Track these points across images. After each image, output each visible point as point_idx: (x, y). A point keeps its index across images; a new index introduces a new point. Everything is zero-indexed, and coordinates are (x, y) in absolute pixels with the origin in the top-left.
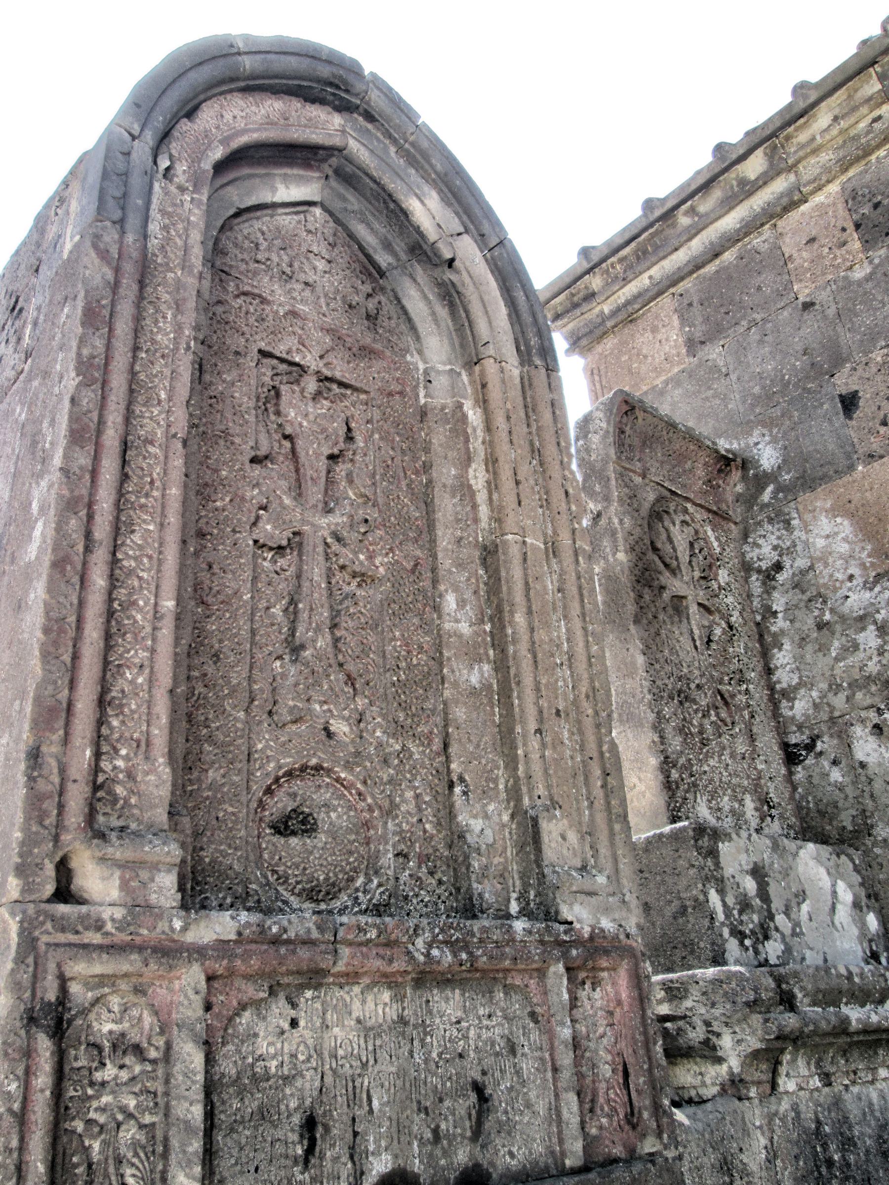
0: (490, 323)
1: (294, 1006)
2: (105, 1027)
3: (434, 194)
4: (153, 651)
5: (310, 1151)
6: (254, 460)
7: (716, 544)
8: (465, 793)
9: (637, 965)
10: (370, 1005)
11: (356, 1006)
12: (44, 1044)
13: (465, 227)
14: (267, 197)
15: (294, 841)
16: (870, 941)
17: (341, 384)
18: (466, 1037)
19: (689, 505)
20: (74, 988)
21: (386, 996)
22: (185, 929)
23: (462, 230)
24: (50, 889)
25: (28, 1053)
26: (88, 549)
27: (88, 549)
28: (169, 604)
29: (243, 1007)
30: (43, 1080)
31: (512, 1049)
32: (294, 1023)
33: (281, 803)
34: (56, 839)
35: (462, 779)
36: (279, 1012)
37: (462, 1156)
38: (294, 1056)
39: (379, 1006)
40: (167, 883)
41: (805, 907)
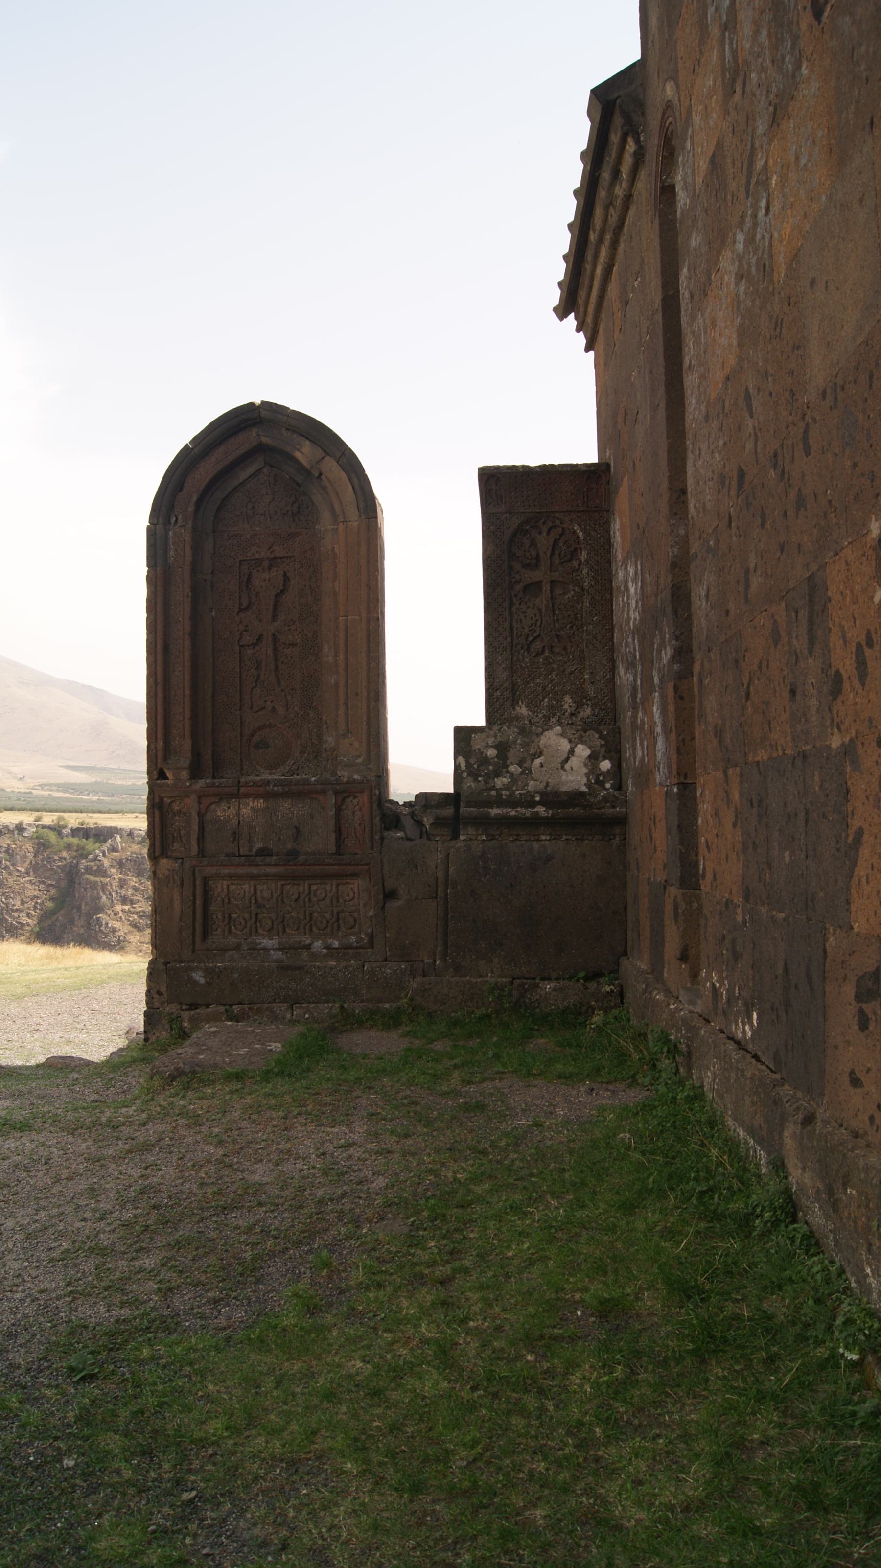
0: (341, 503)
1: (229, 803)
2: (176, 808)
3: (308, 443)
4: (184, 708)
5: (235, 838)
6: (241, 610)
7: (581, 534)
8: (327, 728)
9: (371, 790)
10: (256, 803)
11: (251, 804)
12: (157, 812)
13: (325, 451)
14: (236, 483)
15: (260, 751)
16: (598, 776)
17: (281, 558)
18: (293, 813)
19: (557, 515)
20: (165, 799)
21: (262, 801)
22: (190, 785)
23: (324, 455)
24: (155, 777)
25: (154, 812)
26: (156, 686)
27: (156, 686)
28: (187, 692)
29: (212, 804)
30: (157, 819)
31: (312, 817)
32: (229, 808)
33: (256, 738)
34: (156, 765)
35: (326, 723)
36: (224, 806)
37: (289, 846)
38: (229, 816)
39: (260, 804)
40: (185, 774)
41: (537, 762)
